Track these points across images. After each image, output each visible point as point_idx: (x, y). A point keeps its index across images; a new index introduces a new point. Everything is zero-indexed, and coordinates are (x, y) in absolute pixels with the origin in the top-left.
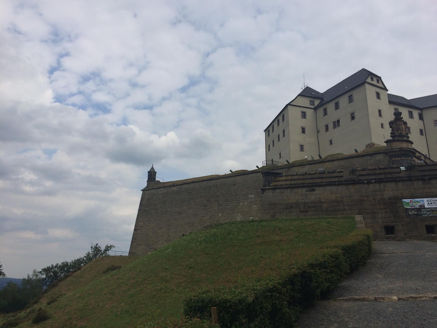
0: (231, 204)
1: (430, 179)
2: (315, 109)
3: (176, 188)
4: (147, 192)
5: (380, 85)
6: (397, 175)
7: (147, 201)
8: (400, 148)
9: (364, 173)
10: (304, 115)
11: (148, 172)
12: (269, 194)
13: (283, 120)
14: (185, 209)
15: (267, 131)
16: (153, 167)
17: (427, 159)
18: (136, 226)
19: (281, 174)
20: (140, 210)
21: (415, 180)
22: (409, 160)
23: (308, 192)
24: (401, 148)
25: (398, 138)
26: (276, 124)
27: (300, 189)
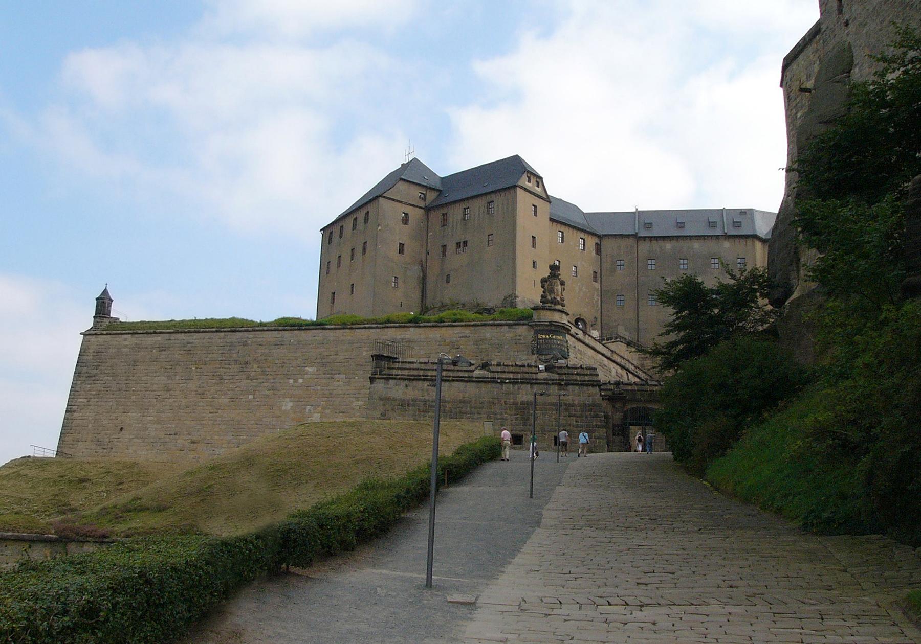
0: (272, 381)
1: (567, 385)
2: (427, 209)
3: (159, 338)
4: (93, 339)
5: (538, 190)
6: (534, 376)
7: (93, 356)
8: (550, 321)
9: (499, 369)
10: (405, 220)
11: (97, 299)
12: (380, 385)
13: (366, 220)
14: (179, 380)
15: (328, 232)
16: (107, 288)
17: (587, 336)
18: (70, 404)
19: (396, 358)
20: (79, 373)
21: (552, 384)
22: (560, 340)
23: (430, 387)
24: (551, 321)
25: (550, 305)
26: (348, 224)
27: (420, 382)
